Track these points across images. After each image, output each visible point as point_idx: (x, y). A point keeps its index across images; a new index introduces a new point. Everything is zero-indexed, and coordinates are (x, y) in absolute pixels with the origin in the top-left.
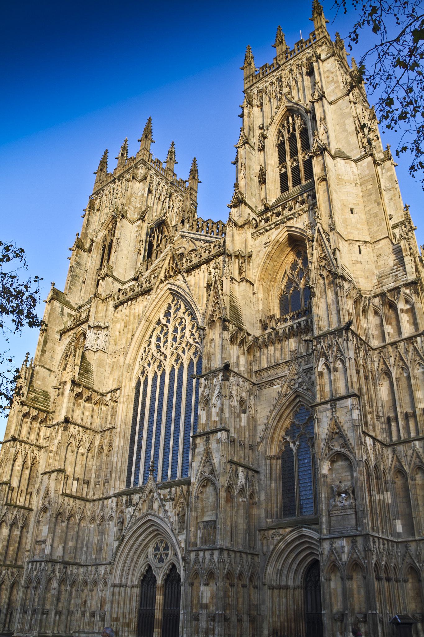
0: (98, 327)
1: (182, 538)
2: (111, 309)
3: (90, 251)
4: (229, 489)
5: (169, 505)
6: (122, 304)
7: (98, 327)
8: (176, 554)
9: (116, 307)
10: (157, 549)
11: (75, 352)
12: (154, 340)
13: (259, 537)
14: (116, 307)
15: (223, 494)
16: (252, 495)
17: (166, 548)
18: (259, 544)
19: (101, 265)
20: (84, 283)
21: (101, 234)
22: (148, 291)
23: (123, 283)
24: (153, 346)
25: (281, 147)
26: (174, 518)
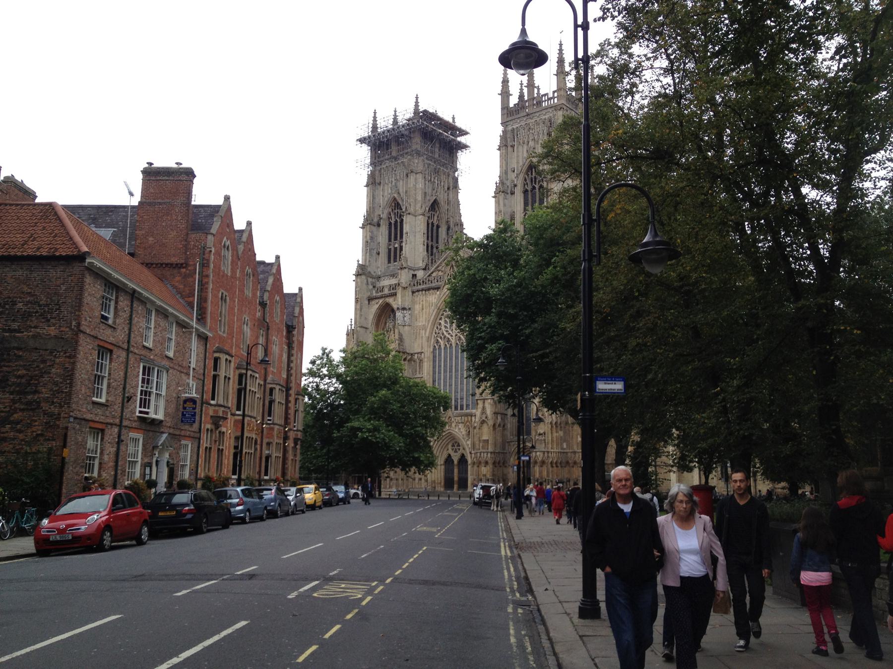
0: (404, 309)
1: (469, 442)
2: (411, 293)
3: (379, 225)
4: (494, 425)
5: (461, 426)
6: (418, 291)
7: (404, 309)
8: (464, 449)
9: (413, 292)
10: (453, 446)
11: (394, 331)
12: (442, 322)
13: (507, 445)
14: (413, 292)
15: (492, 428)
16: (504, 426)
17: (459, 445)
18: (507, 448)
19: (390, 240)
20: (379, 254)
21: (386, 212)
22: (438, 288)
23: (414, 270)
24: (443, 328)
25: (525, 192)
26: (464, 433)
